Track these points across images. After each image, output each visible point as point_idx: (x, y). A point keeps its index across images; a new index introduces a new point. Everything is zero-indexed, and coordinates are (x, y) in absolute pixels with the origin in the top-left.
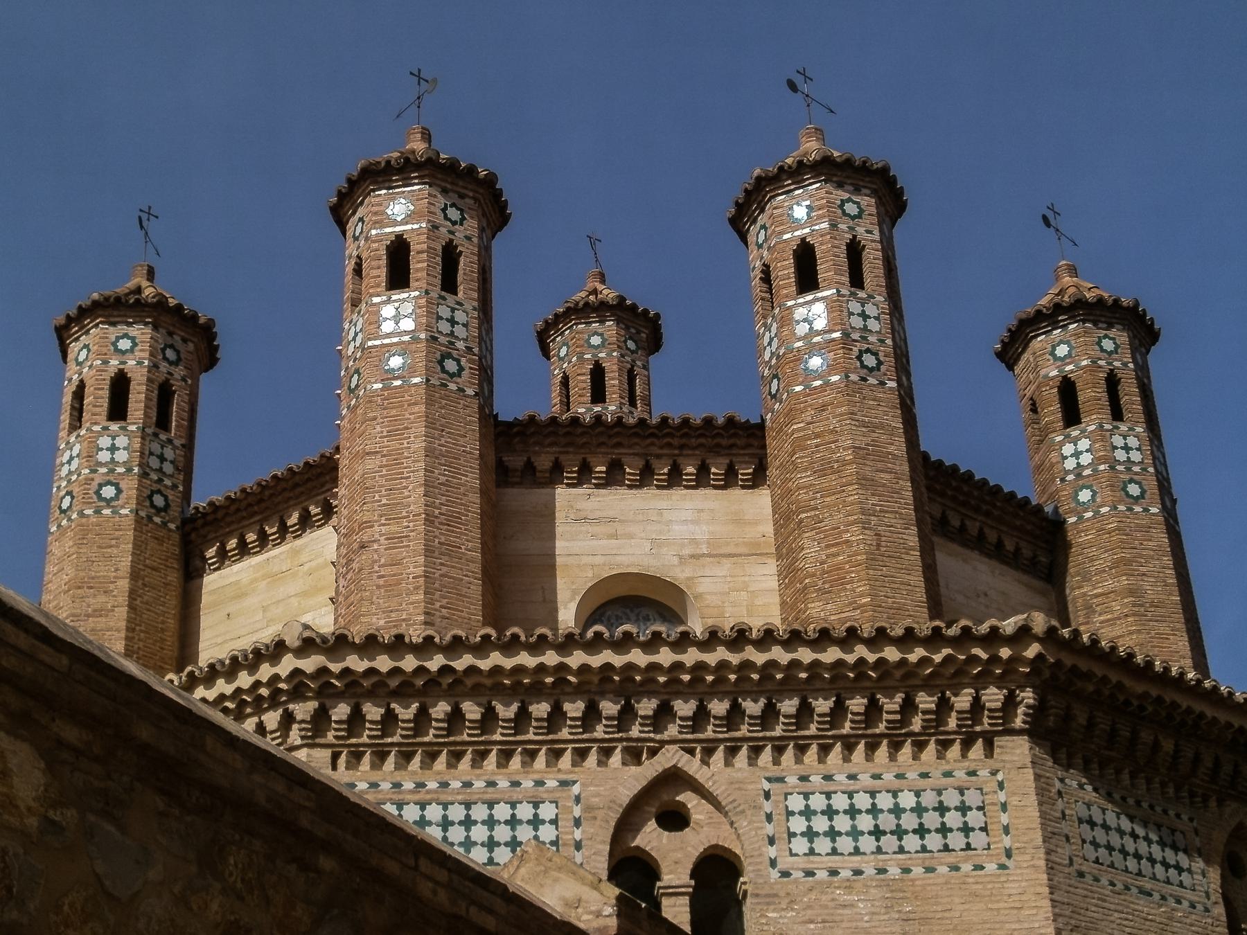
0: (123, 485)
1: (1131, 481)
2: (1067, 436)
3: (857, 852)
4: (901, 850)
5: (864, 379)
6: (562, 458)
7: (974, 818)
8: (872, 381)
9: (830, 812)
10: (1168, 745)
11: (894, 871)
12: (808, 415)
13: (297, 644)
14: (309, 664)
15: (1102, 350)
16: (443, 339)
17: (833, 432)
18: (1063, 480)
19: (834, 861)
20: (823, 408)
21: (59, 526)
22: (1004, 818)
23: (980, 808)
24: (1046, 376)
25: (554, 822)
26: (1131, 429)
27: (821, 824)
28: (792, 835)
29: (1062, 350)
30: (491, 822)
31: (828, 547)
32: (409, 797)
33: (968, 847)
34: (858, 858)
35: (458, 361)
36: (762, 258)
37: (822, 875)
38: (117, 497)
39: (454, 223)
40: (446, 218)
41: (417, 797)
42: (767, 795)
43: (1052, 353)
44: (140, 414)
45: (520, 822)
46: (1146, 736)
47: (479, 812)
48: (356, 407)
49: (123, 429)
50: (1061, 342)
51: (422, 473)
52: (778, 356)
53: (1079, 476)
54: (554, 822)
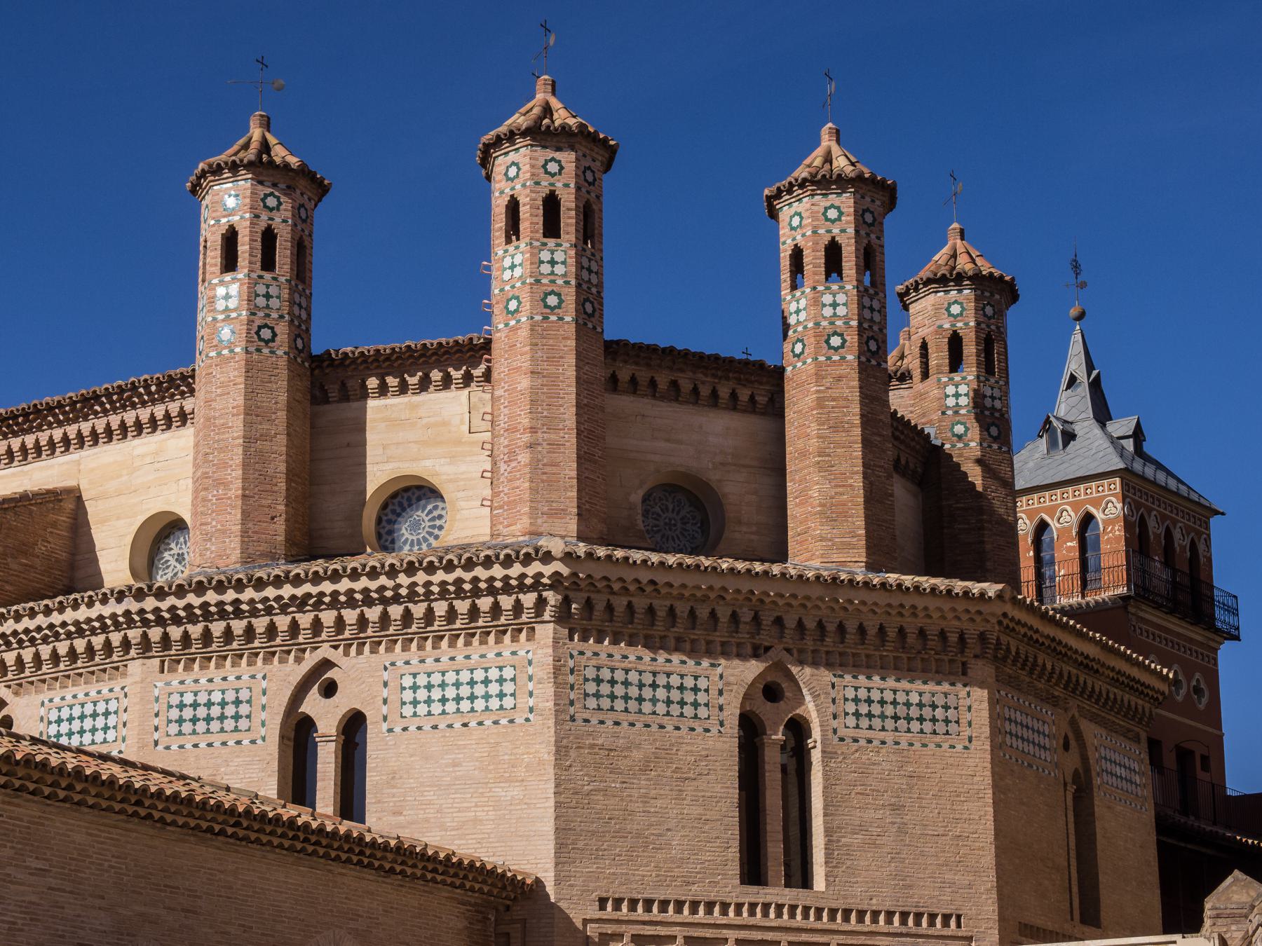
0: (277, 330)
1: (993, 424)
2: (951, 379)
3: (883, 729)
4: (909, 731)
5: (869, 361)
6: (637, 374)
7: (951, 714)
8: (873, 362)
9: (869, 701)
10: (1049, 667)
11: (904, 745)
12: (828, 381)
13: (560, 556)
14: (565, 571)
15: (985, 315)
16: (585, 286)
17: (846, 399)
18: (944, 413)
19: (870, 734)
20: (839, 379)
21: (219, 354)
22: (969, 716)
23: (956, 708)
24: (940, 327)
25: (707, 691)
26: (997, 382)
27: (864, 709)
28: (847, 714)
29: (955, 309)
30: (668, 687)
31: (836, 486)
32: (617, 665)
33: (947, 733)
34: (883, 733)
35: (592, 303)
36: (794, 239)
37: (863, 743)
38: (273, 340)
39: (590, 184)
40: (586, 180)
41: (623, 665)
42: (833, 687)
43: (948, 310)
44: (287, 267)
45: (686, 688)
46: (1040, 661)
47: (662, 680)
48: (514, 330)
49: (275, 279)
50: (956, 302)
51: (574, 396)
52: (805, 327)
53: (956, 413)
54: (707, 691)
